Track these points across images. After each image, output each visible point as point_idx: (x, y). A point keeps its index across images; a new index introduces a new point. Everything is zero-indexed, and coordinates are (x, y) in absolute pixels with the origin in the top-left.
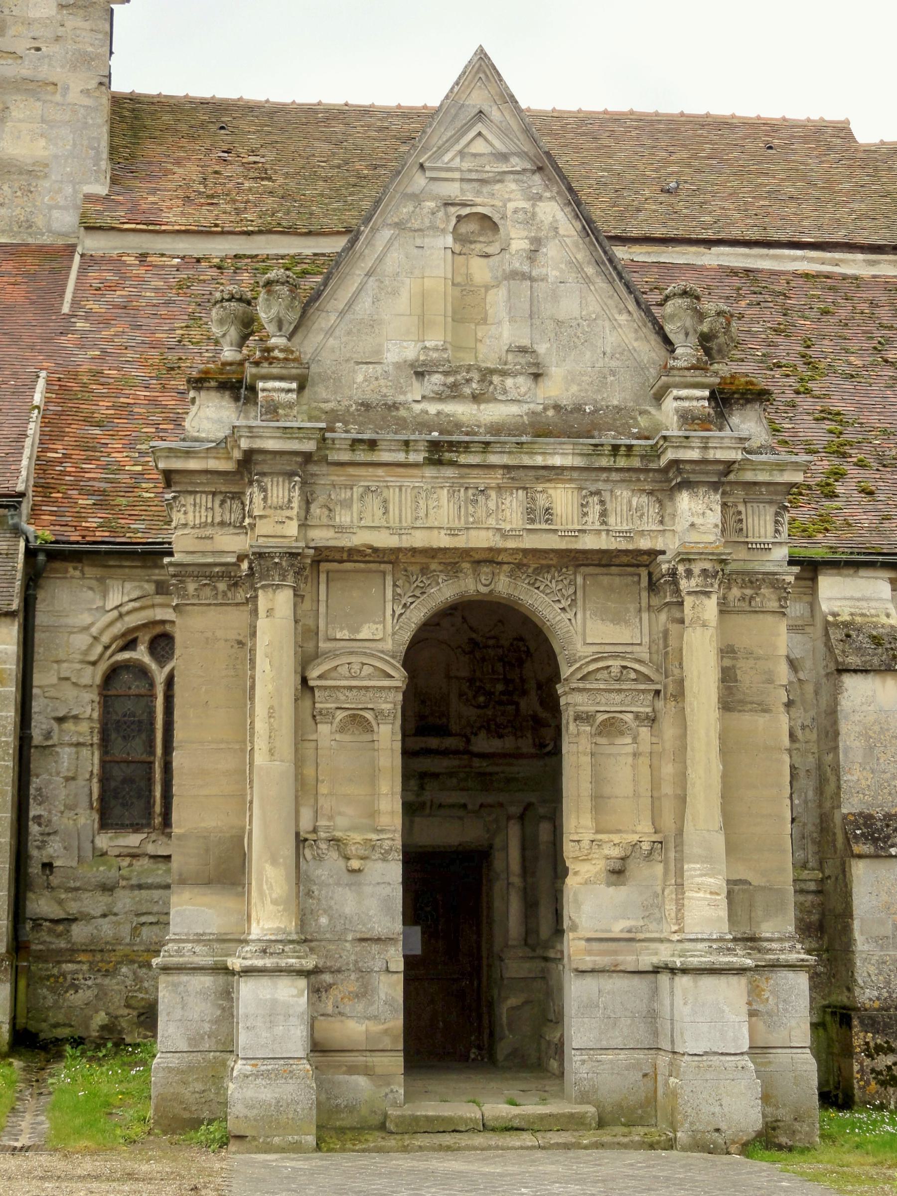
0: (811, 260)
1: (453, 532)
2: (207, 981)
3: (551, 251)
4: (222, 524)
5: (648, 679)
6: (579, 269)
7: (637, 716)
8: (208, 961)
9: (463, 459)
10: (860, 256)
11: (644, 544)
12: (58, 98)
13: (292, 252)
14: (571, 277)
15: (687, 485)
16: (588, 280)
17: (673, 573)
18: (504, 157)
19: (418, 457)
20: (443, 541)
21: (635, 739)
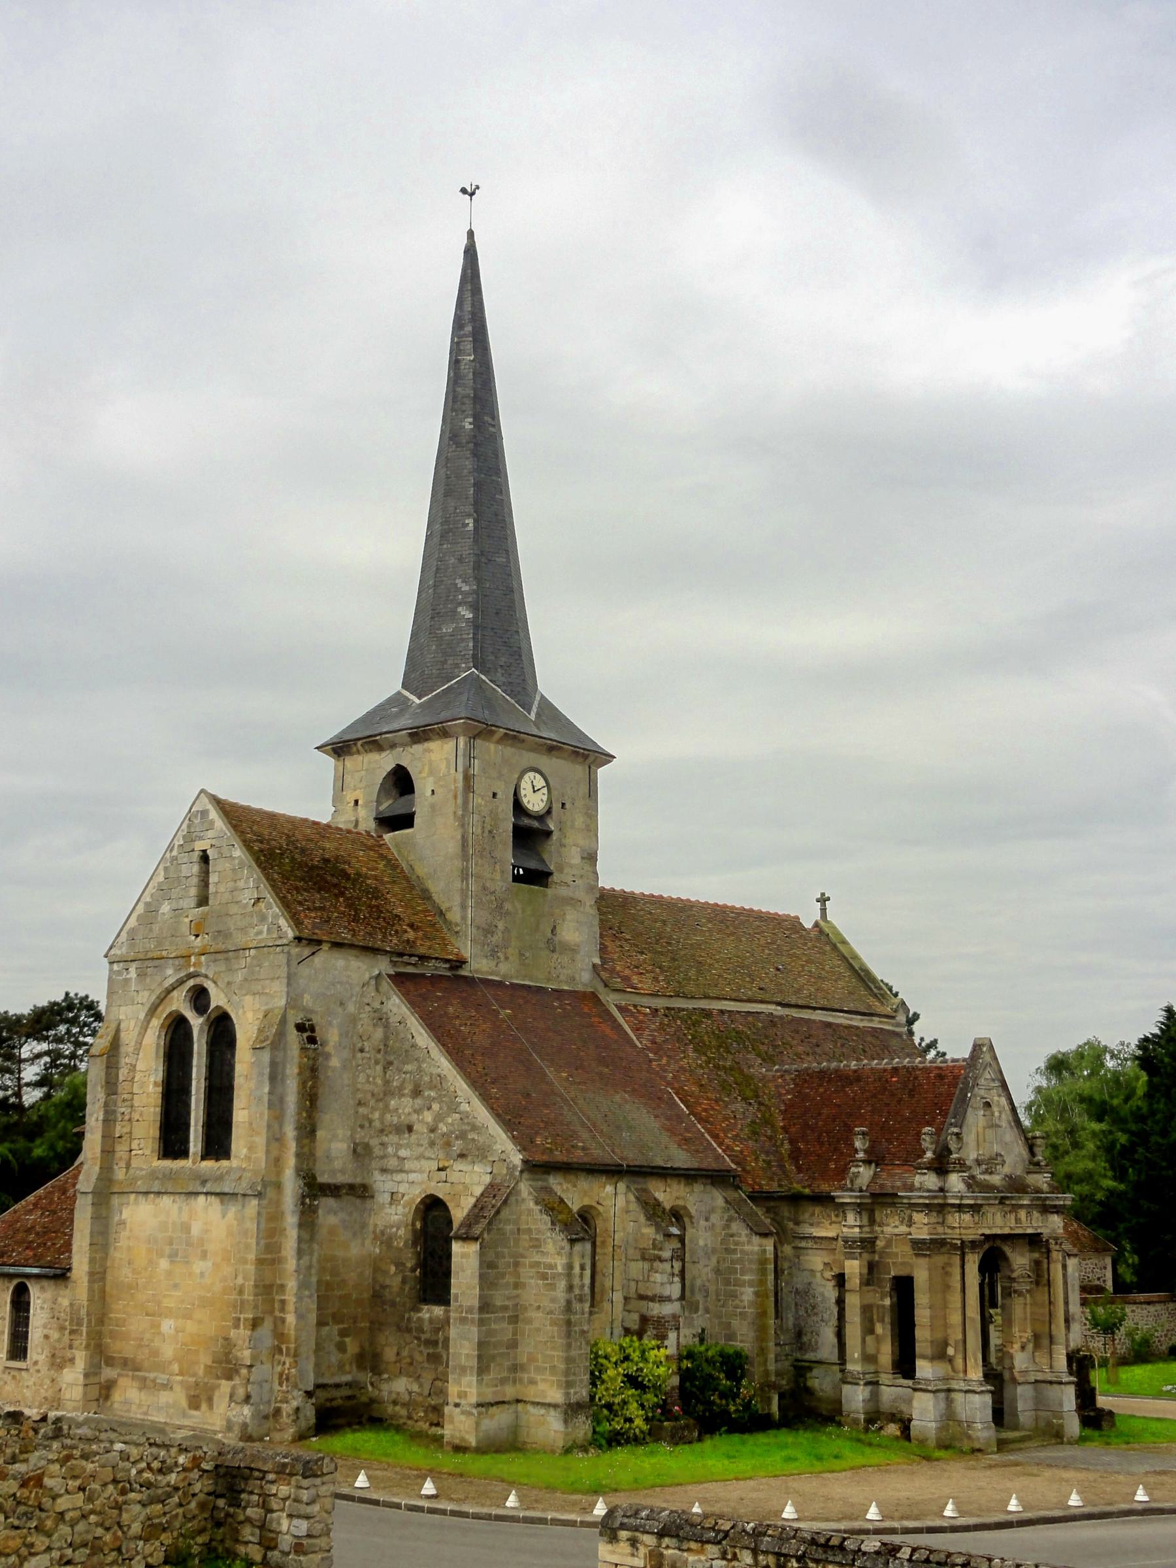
0: (848, 1019)
1: (1001, 1227)
2: (942, 1395)
3: (1003, 1116)
4: (938, 1223)
5: (1029, 1276)
6: (1010, 1123)
7: (1027, 1290)
8: (945, 1387)
9: (1007, 1202)
10: (859, 1017)
11: (1039, 1231)
12: (582, 909)
13: (685, 1006)
14: (1008, 1126)
15: (1057, 1212)
16: (1011, 1127)
17: (1047, 1241)
18: (993, 1080)
19: (997, 1202)
20: (999, 1232)
21: (1025, 1298)
